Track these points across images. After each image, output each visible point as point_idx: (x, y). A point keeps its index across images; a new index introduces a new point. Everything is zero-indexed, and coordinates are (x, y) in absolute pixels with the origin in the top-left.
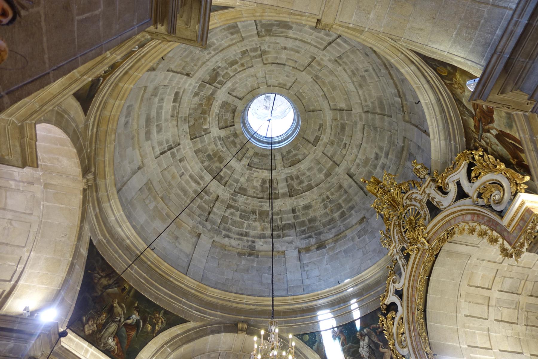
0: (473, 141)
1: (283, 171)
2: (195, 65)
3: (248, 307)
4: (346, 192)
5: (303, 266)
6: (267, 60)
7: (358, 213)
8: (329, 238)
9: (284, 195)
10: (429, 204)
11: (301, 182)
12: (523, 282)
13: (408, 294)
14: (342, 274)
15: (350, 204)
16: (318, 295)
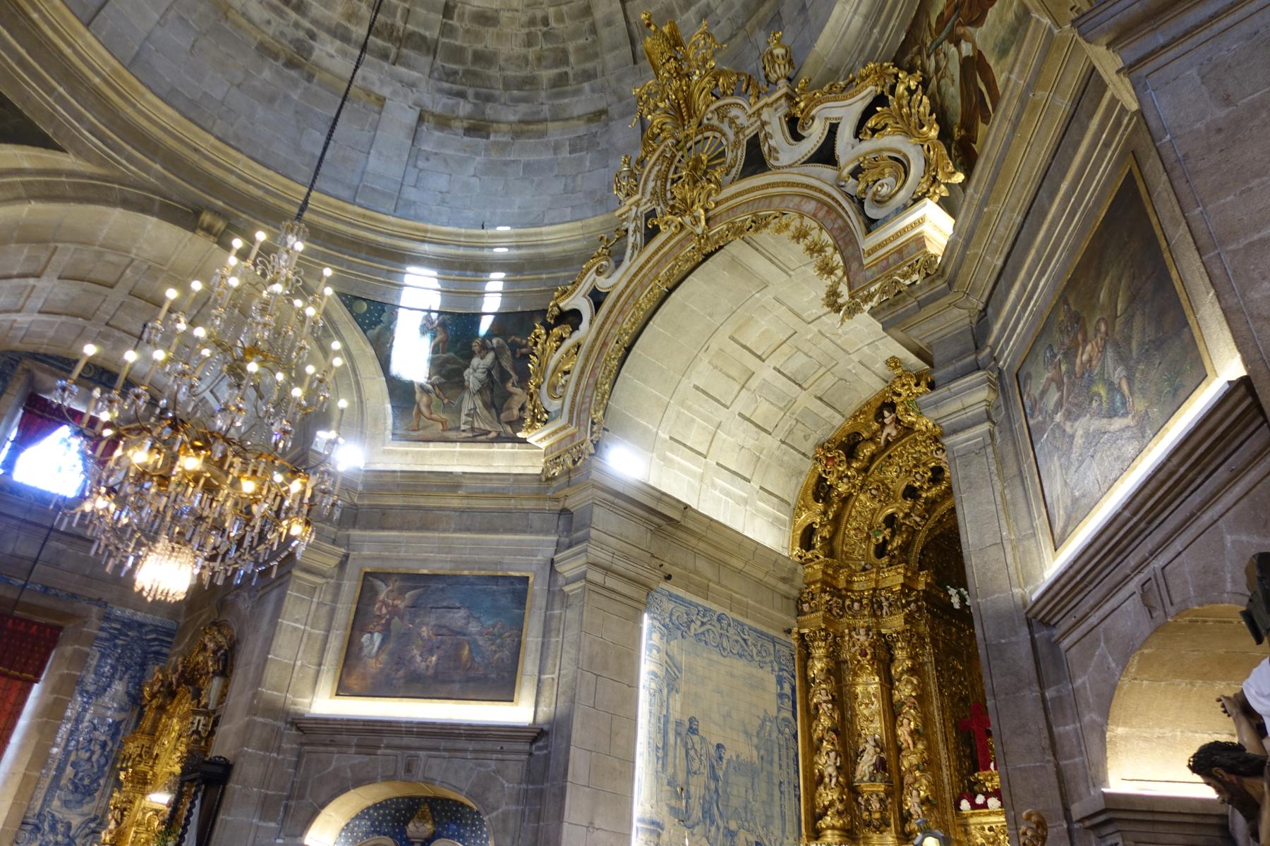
0: (915, 49)
3: (243, 186)
4: (593, 30)
5: (415, 154)
7: (596, 95)
8: (503, 118)
10: (754, 145)
13: (614, 306)
14: (498, 211)
15: (588, 65)
16: (426, 231)
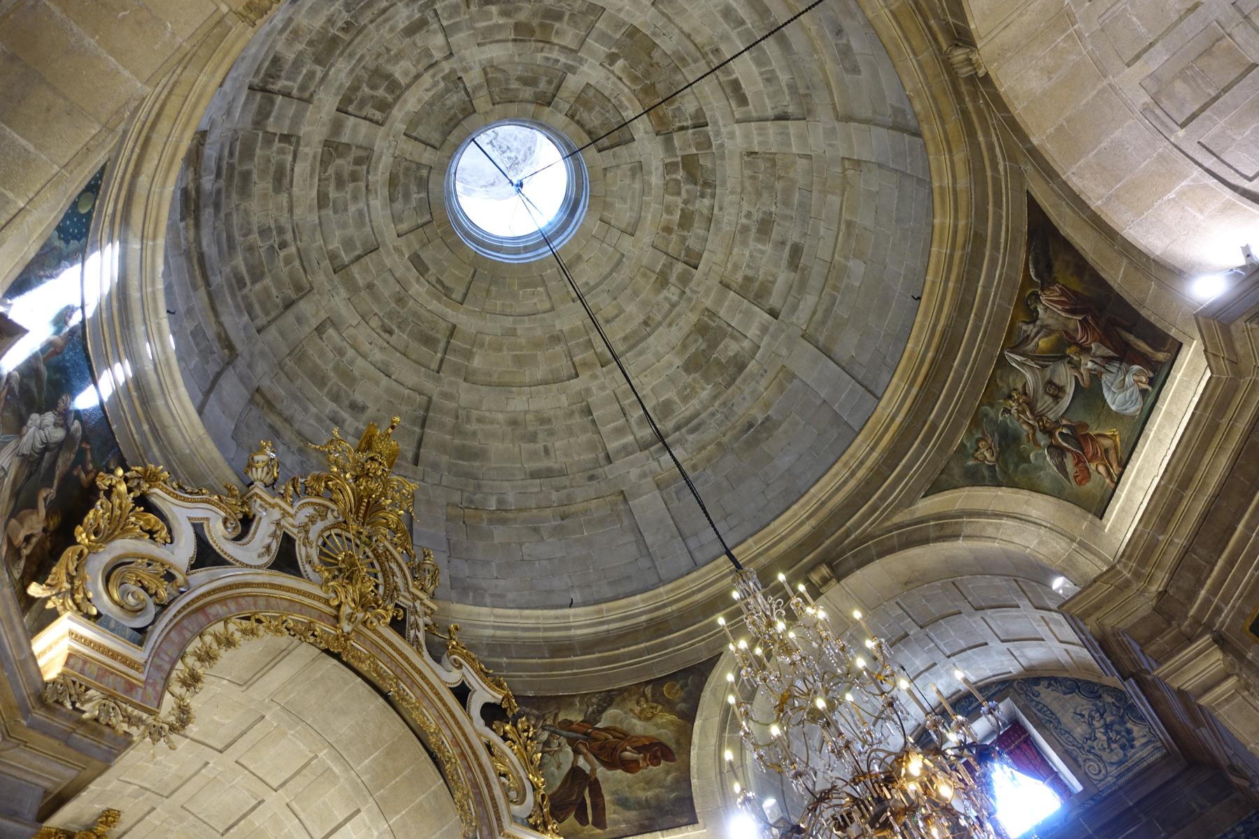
1: (391, 151)
2: (753, 178)
6: (644, 275)
9: (337, 127)
11: (340, 184)
15: (257, 307)
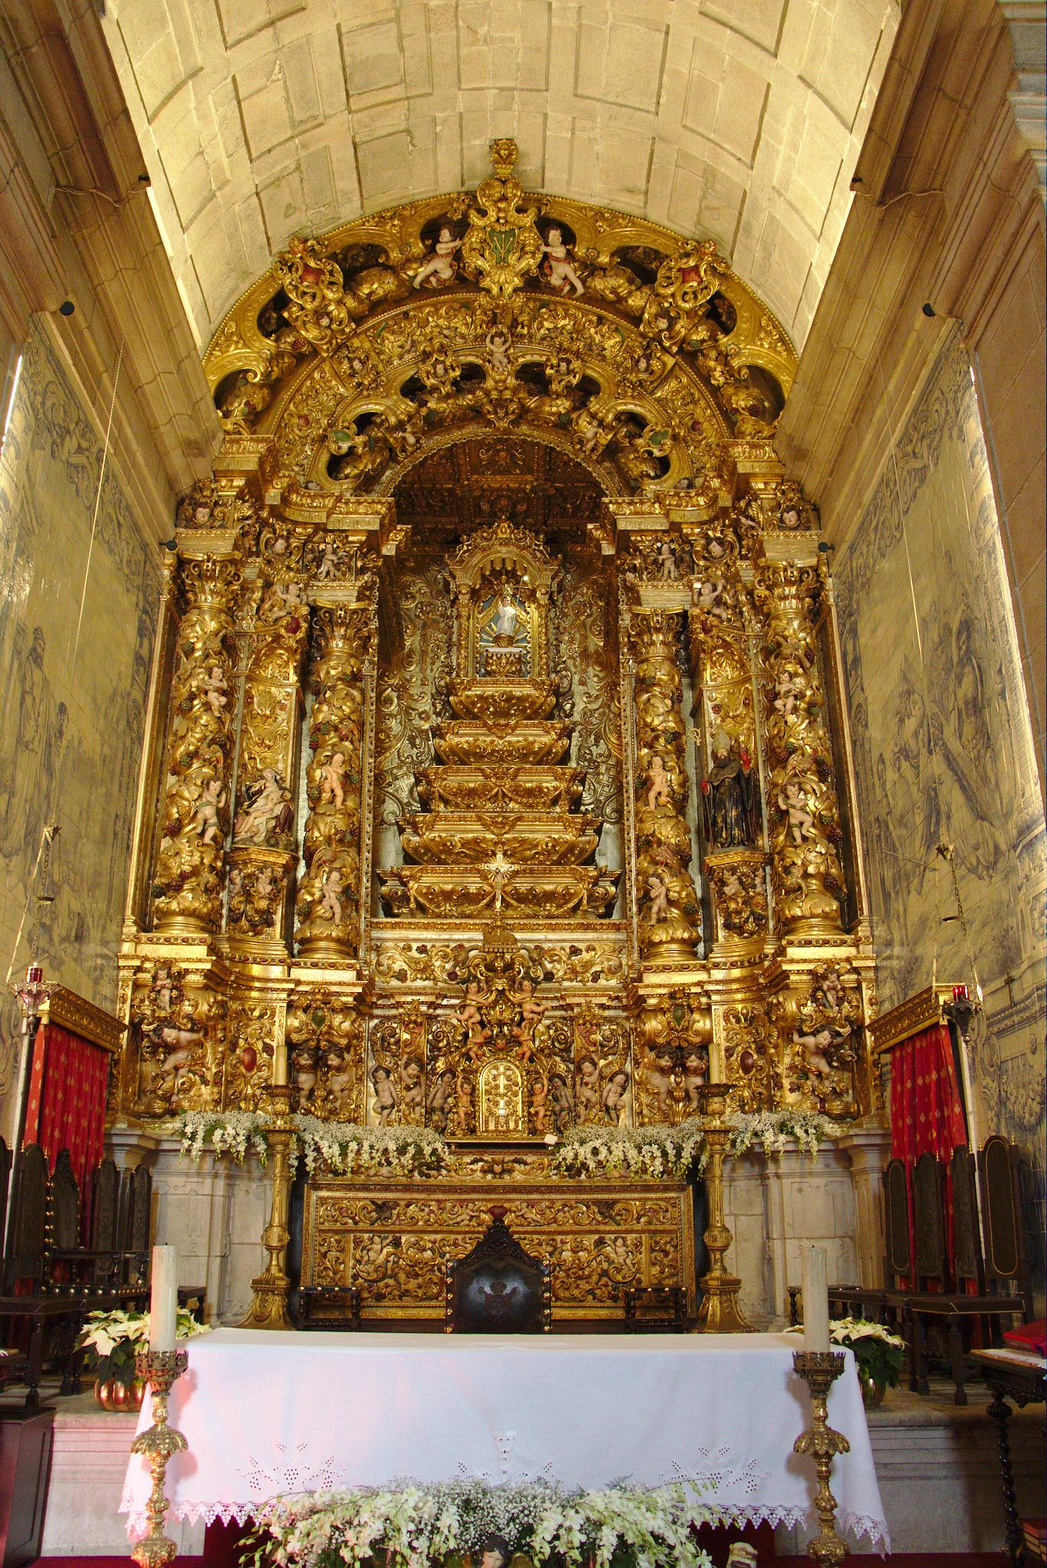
12: (397, 92)
